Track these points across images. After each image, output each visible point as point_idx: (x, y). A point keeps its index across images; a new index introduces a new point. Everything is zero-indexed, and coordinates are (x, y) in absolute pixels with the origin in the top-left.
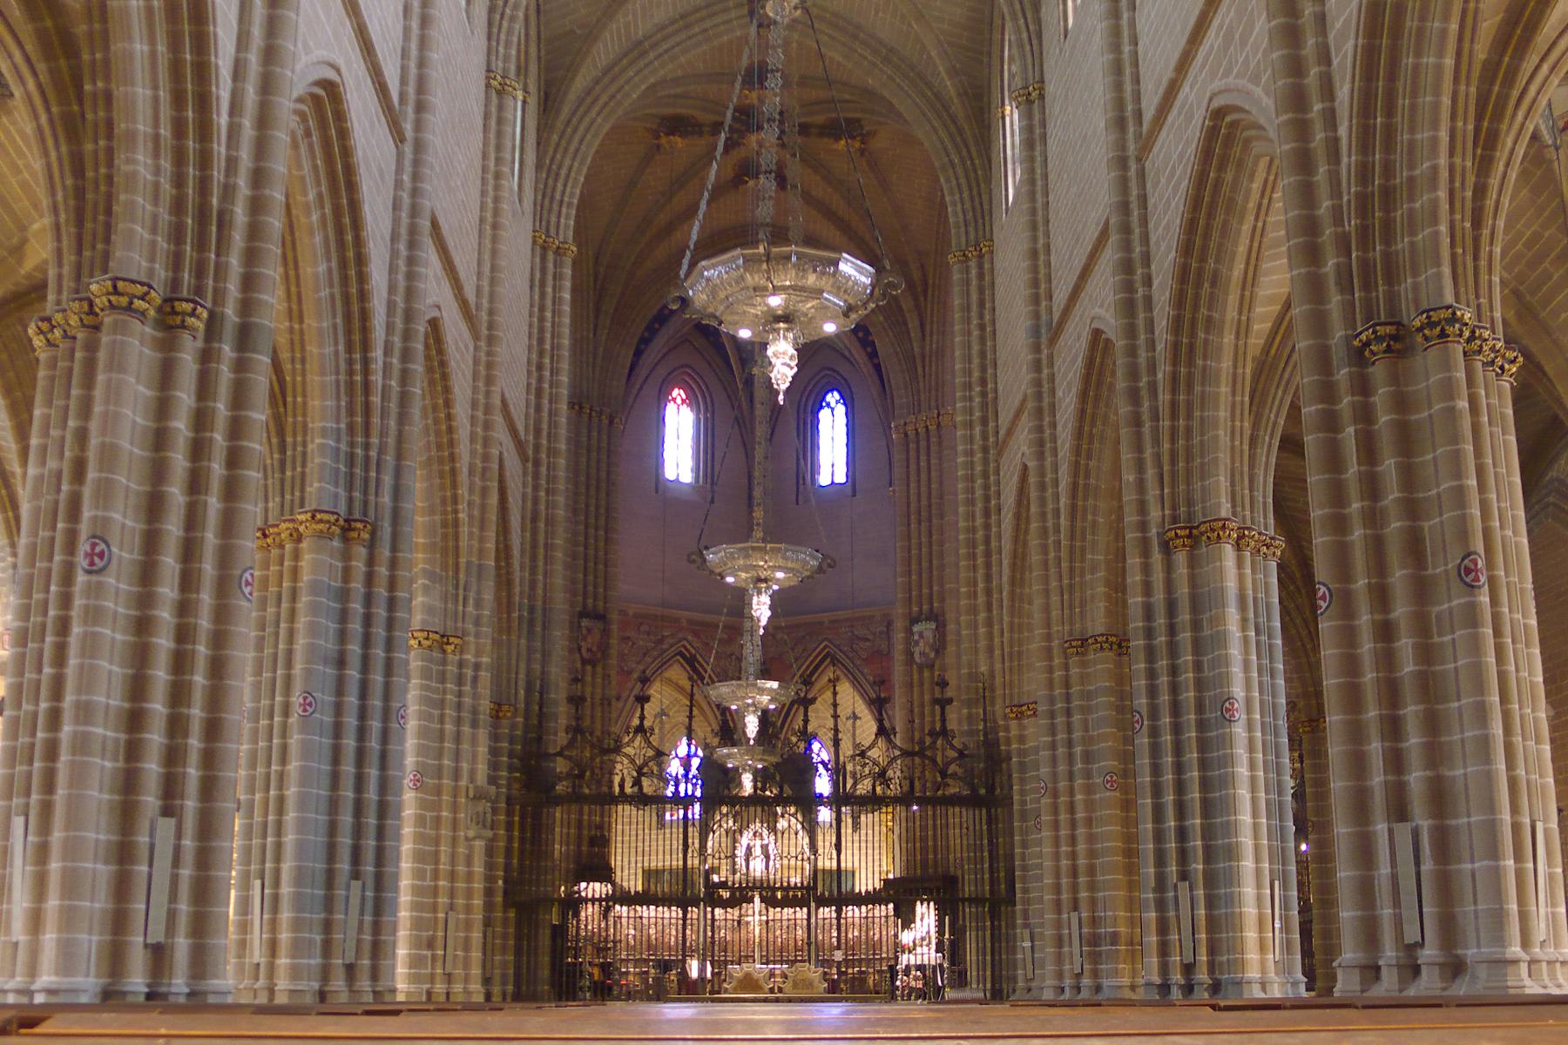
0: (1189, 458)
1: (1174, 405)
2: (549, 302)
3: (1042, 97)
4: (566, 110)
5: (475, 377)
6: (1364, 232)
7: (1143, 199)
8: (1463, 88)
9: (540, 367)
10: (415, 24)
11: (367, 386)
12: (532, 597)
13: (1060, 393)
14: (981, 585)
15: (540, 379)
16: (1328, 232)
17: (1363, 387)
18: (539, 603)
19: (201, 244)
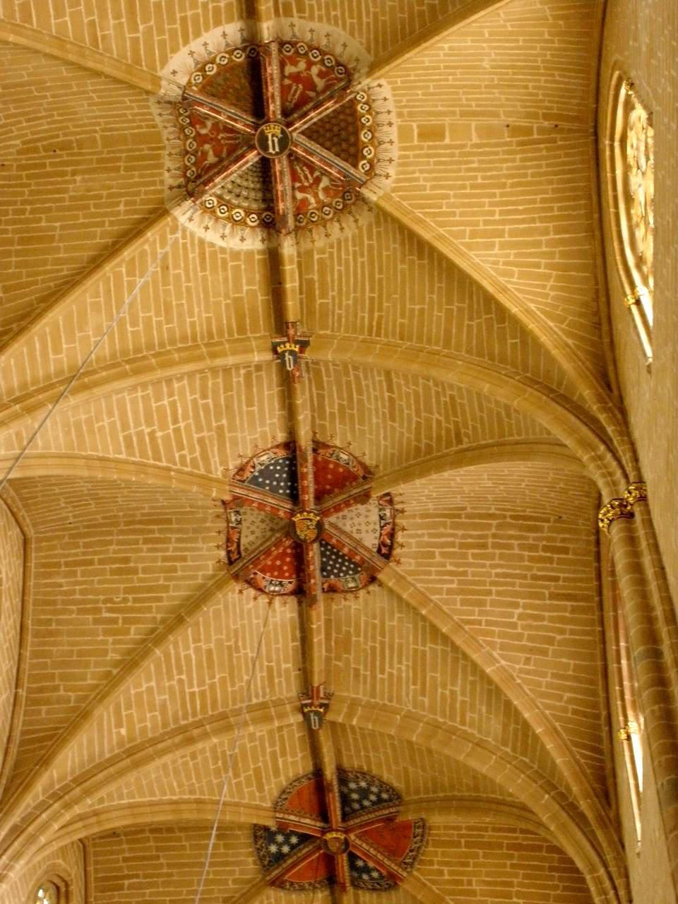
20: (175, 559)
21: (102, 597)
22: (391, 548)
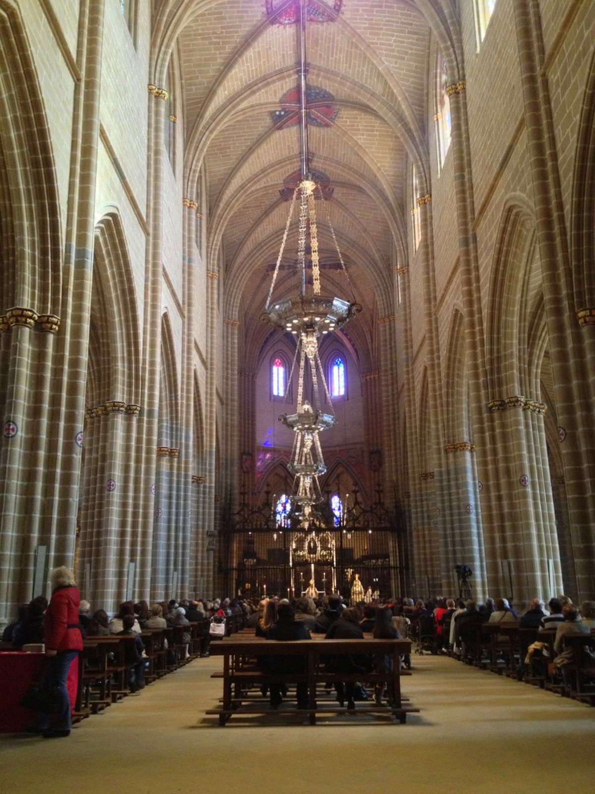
0: (453, 420)
1: (448, 402)
2: (230, 344)
3: (408, 271)
4: (234, 271)
5: (207, 383)
6: (492, 370)
7: (437, 328)
8: (522, 324)
9: (227, 369)
10: (186, 276)
11: (176, 404)
12: (226, 455)
13: (416, 383)
14: (393, 447)
15: (227, 373)
16: (481, 369)
17: (492, 420)
18: (229, 457)
19: (137, 387)
20: (243, 12)
21: (211, 31)
22: (340, 7)
